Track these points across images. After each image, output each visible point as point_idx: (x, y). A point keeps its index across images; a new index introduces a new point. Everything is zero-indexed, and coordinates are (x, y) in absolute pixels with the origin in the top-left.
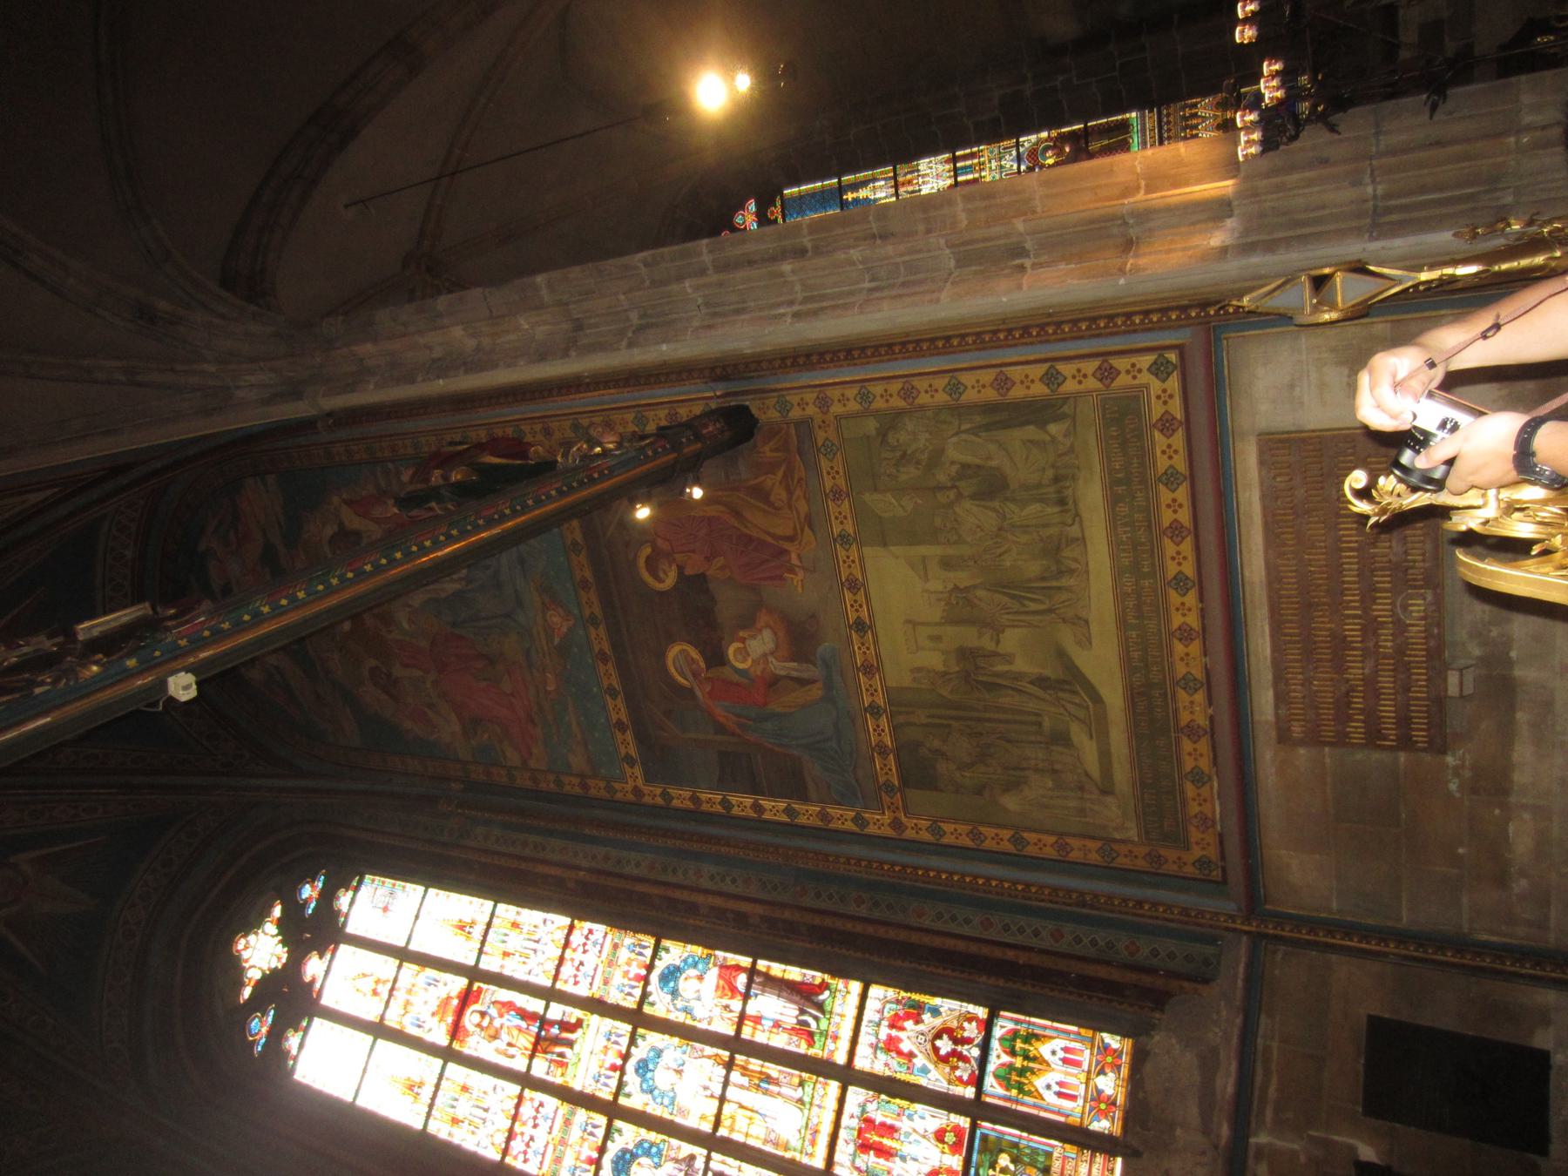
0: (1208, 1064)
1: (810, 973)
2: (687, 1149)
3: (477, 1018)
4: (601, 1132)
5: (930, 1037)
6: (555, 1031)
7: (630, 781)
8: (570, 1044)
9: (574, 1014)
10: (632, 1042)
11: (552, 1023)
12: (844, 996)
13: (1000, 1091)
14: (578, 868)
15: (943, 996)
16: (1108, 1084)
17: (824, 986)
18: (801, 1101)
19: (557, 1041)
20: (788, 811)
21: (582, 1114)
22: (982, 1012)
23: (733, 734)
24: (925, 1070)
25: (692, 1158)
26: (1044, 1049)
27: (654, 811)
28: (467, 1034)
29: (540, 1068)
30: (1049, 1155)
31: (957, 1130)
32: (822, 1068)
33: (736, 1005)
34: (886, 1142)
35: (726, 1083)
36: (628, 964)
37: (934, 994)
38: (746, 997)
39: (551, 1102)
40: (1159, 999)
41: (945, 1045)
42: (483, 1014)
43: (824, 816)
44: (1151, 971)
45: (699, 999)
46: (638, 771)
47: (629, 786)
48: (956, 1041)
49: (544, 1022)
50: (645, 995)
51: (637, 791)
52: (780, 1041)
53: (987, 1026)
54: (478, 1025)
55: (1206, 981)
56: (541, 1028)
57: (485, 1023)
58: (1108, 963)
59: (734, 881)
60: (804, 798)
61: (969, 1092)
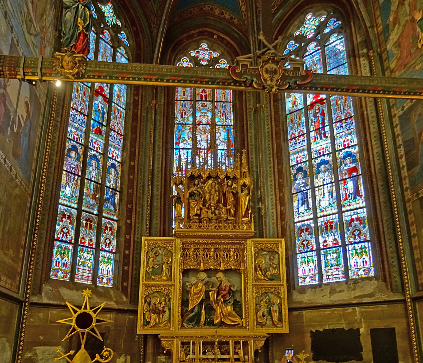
0: (371, 295)
1: (363, 191)
2: (309, 183)
3: (317, 108)
4: (304, 160)
5: (357, 228)
6: (323, 132)
7: (397, 112)
8: (321, 138)
9: (328, 135)
10: (328, 154)
11: (324, 130)
12: (361, 202)
13: (350, 249)
14: (367, 110)
15: (369, 228)
16: (361, 273)
17: (361, 196)
18: (330, 204)
19: (320, 134)
20: (403, 166)
21: (306, 152)
22: (368, 238)
23: (420, 139)
24: (348, 230)
25: (308, 185)
26: (364, 256)
27: (392, 123)
28: (312, 108)
29: (312, 134)
30: (340, 264)
31: (338, 243)
32: (340, 206)
33: (347, 176)
34: (329, 228)
35: (327, 184)
36: (348, 140)
37: (368, 225)
38: (350, 178)
39: (305, 143)
40: (385, 280)
41: (357, 233)
42: (319, 109)
43: (405, 178)
44: (390, 277)
45: (345, 165)
46: (401, 112)
47: (396, 112)
48: (358, 235)
49: (323, 128)
50: (341, 150)
51: (395, 115)
52: (342, 192)
53: (365, 241)
54: (316, 110)
55: (392, 290)
56: (322, 128)
57: (317, 111)
58: (389, 267)
59: (378, 160)
60: (409, 170)
61: (347, 243)
